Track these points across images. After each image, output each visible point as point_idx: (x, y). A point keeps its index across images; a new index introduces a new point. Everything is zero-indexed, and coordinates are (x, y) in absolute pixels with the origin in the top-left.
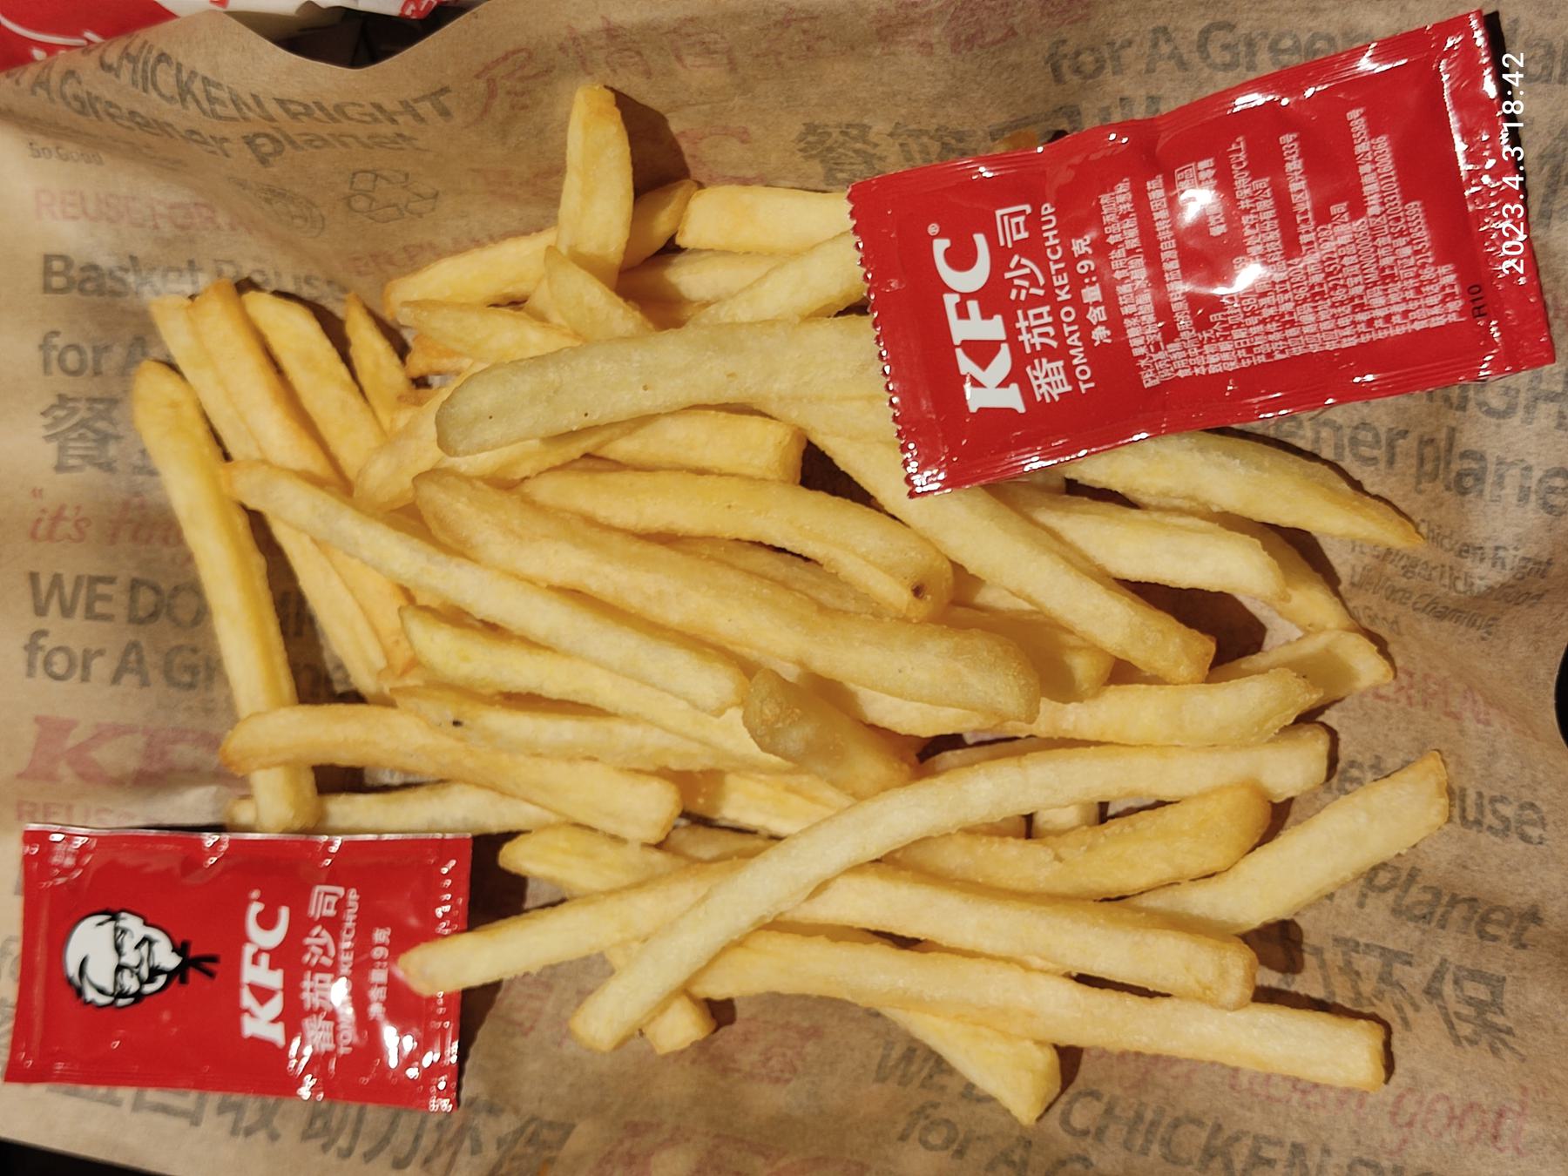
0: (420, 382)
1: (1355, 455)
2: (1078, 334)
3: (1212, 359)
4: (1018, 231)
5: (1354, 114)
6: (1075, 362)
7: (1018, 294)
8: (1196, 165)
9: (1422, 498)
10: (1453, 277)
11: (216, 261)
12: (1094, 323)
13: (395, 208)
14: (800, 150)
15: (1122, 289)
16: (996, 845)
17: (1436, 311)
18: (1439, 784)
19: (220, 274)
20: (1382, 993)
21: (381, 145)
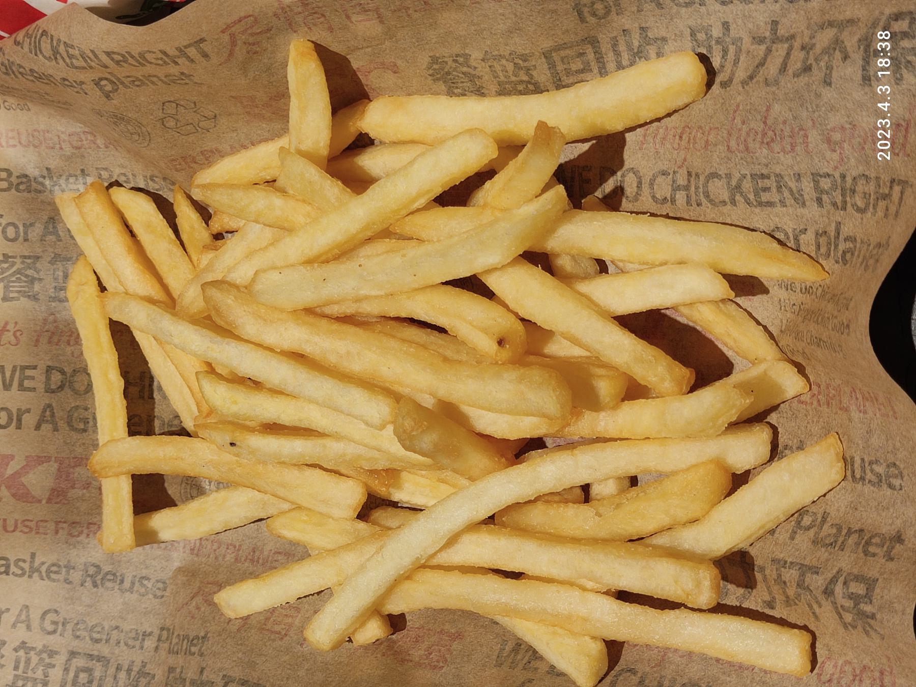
0: (218, 236)
11: (97, 169)
13: (192, 126)
14: (430, 75)
16: (562, 509)
18: (837, 454)
19: (100, 176)
20: (799, 595)
21: (174, 82)
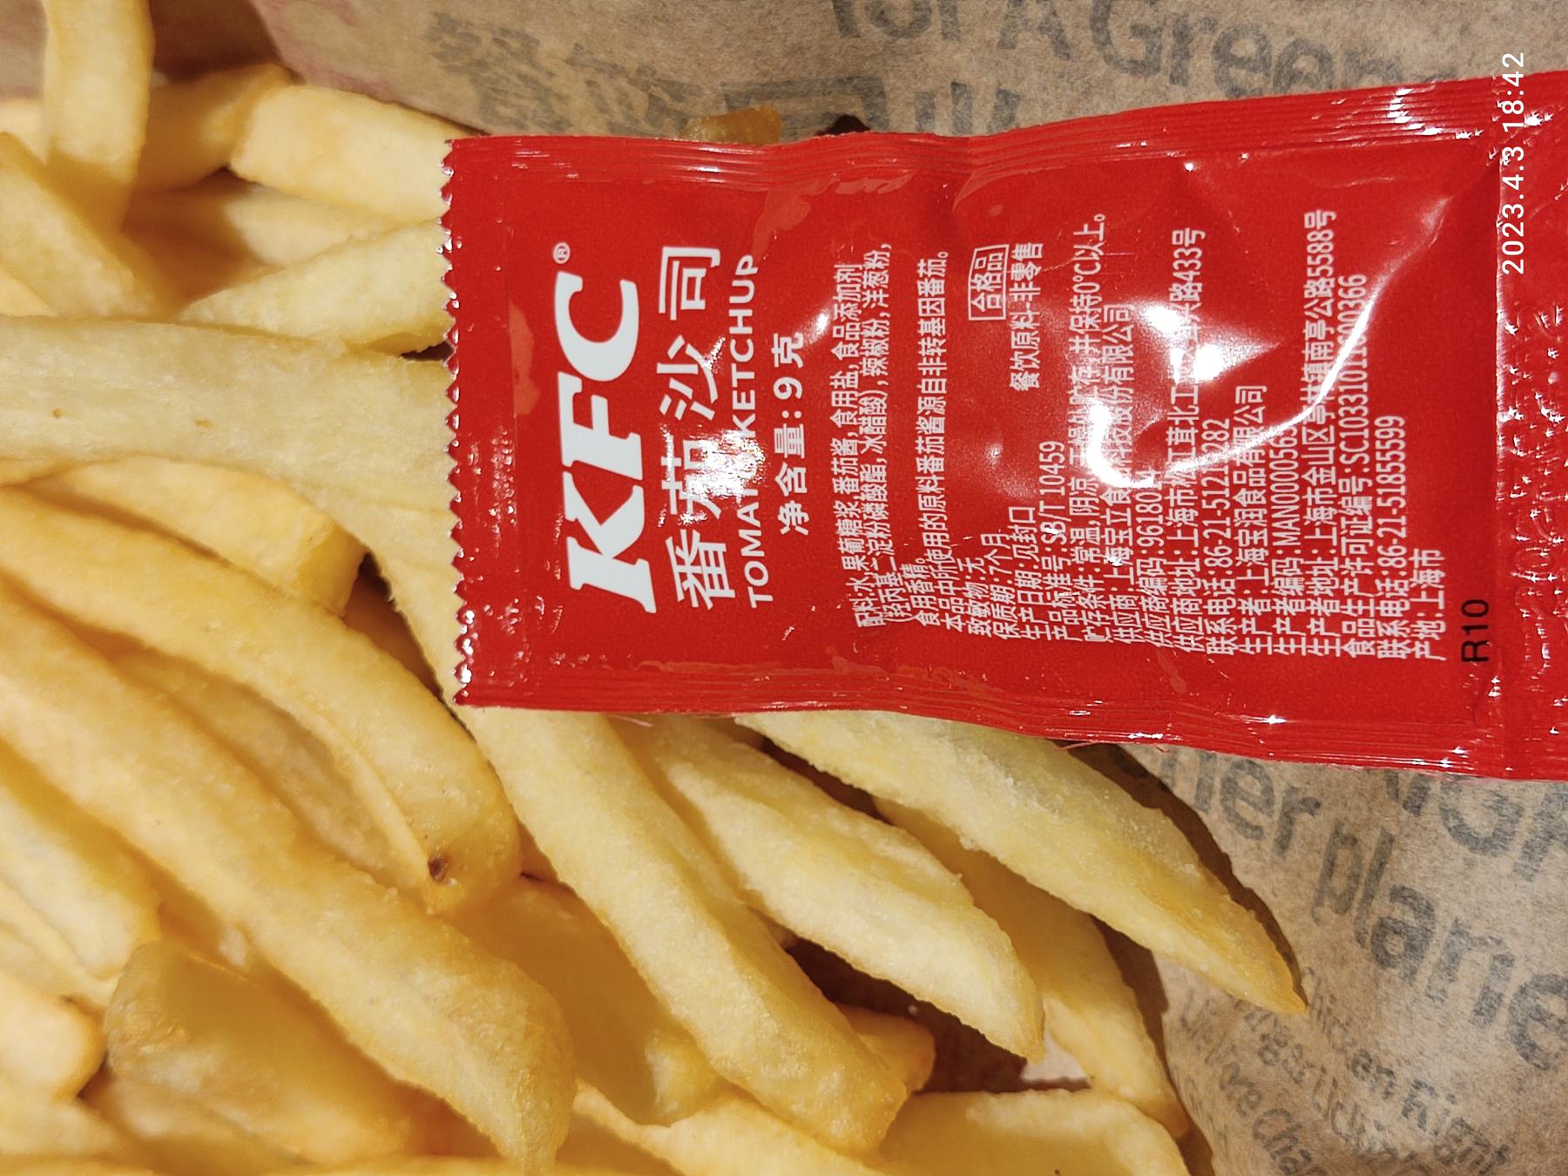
1: (1227, 809)
2: (756, 506)
3: (977, 610)
4: (691, 296)
5: (1316, 219)
6: (746, 552)
7: (673, 408)
8: (1012, 248)
9: (1318, 931)
10: (1439, 574)
12: (786, 494)
15: (843, 447)
17: (1394, 629)
